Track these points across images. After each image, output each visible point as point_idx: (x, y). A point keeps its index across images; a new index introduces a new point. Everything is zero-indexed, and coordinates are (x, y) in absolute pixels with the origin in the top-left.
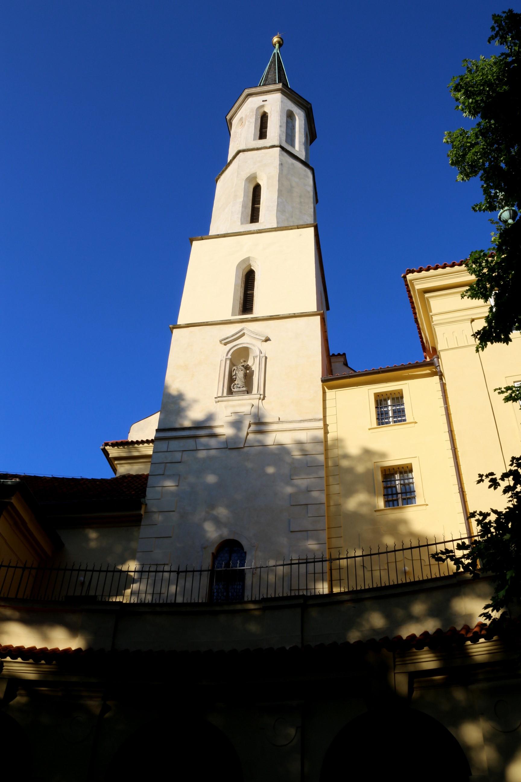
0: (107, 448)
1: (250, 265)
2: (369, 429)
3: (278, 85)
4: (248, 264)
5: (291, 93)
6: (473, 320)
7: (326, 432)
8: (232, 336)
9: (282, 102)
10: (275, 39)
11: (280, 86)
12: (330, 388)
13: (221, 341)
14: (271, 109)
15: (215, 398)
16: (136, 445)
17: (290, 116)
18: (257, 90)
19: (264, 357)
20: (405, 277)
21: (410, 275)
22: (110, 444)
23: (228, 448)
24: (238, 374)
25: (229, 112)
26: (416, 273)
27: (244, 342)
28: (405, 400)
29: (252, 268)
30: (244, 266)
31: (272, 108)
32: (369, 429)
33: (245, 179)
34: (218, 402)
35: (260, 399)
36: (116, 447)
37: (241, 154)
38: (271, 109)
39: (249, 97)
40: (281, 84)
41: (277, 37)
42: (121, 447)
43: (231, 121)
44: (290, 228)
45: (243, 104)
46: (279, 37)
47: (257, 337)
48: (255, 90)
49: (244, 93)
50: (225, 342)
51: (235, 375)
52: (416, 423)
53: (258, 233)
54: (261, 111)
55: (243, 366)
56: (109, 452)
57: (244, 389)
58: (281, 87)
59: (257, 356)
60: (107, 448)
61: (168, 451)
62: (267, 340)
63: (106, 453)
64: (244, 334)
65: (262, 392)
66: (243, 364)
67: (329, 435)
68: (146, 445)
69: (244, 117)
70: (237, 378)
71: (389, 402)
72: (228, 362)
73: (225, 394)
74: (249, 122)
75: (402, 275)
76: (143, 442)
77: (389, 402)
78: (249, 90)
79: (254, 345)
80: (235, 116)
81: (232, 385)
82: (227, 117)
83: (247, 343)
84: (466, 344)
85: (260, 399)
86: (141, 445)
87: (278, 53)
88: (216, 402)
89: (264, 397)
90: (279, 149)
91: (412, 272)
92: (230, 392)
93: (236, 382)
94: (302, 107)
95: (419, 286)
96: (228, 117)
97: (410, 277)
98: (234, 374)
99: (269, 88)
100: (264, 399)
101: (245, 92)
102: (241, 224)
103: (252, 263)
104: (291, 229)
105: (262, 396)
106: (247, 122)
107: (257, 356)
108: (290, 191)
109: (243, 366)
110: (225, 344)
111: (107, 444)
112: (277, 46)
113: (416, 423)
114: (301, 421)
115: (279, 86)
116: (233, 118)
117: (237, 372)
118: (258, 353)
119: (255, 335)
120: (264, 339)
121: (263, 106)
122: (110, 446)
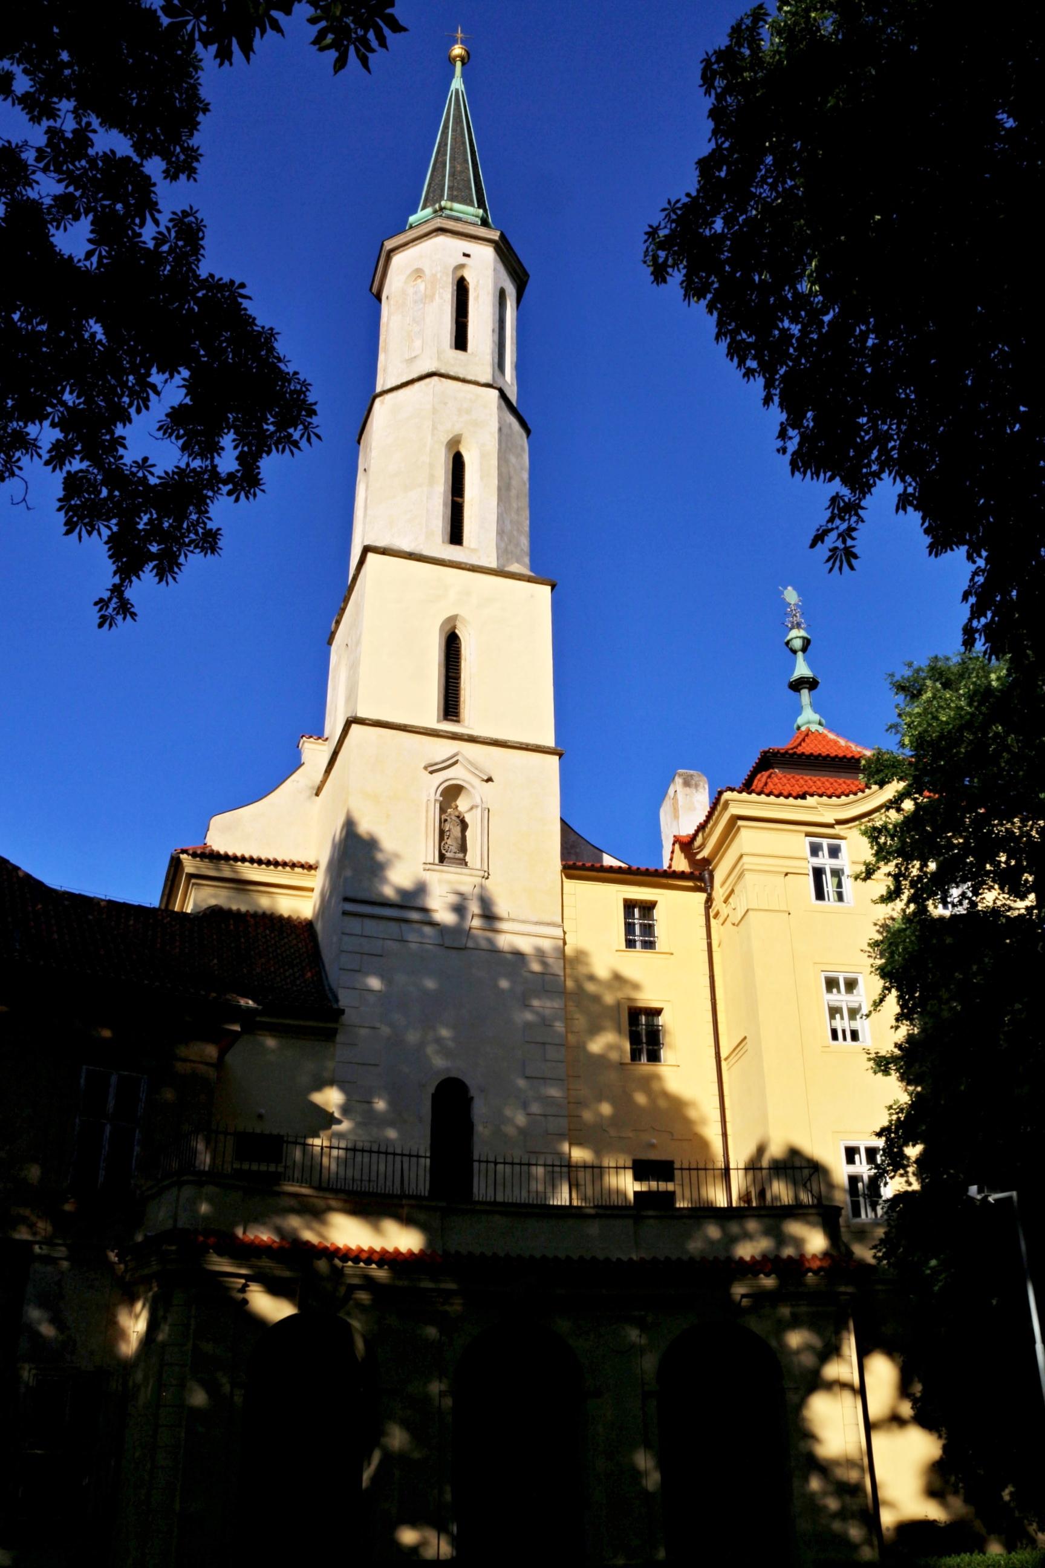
0: (183, 856)
1: (455, 627)
2: (617, 951)
3: (493, 233)
4: (452, 625)
5: (508, 250)
6: (786, 874)
7: (565, 943)
8: (443, 762)
9: (495, 270)
10: (457, 50)
11: (496, 235)
12: (569, 877)
13: (426, 768)
14: (478, 282)
15: (424, 863)
16: (232, 862)
17: (502, 295)
18: (458, 227)
19: (487, 810)
20: (720, 793)
21: (729, 793)
22: (191, 852)
23: (446, 945)
24: (453, 830)
25: (392, 237)
26: (735, 793)
27: (457, 775)
28: (657, 913)
29: (457, 631)
30: (448, 628)
31: (481, 282)
32: (617, 951)
33: (445, 443)
34: (428, 870)
35: (483, 877)
36: (198, 859)
37: (436, 378)
38: (478, 282)
39: (439, 232)
40: (498, 233)
41: (462, 48)
42: (207, 860)
43: (392, 254)
44: (518, 577)
45: (425, 238)
46: (465, 50)
47: (477, 772)
48: (454, 226)
49: (433, 223)
50: (433, 769)
51: (449, 831)
52: (672, 954)
53: (469, 570)
54: (459, 274)
55: (458, 817)
56: (185, 864)
57: (461, 855)
58: (497, 238)
59: (477, 806)
60: (183, 856)
61: (364, 934)
62: (489, 780)
63: (176, 864)
64: (456, 762)
65: (486, 869)
66: (457, 814)
67: (566, 947)
68: (247, 864)
69: (427, 272)
70: (451, 836)
71: (636, 911)
72: (438, 805)
73: (437, 861)
74: (441, 298)
75: (719, 790)
76: (243, 859)
77: (636, 911)
78: (444, 221)
79: (473, 787)
80: (401, 249)
81: (442, 844)
82: (386, 243)
83: (464, 780)
84: (778, 909)
85: (483, 877)
86: (239, 863)
87: (462, 91)
88: (424, 870)
89: (489, 874)
90: (496, 393)
91: (732, 790)
92: (442, 858)
93: (449, 842)
94: (515, 277)
95: (734, 810)
96: (389, 244)
97: (727, 795)
98: (447, 829)
99: (477, 231)
100: (487, 878)
101: (435, 221)
102: (443, 542)
103: (459, 625)
104: (519, 580)
105: (486, 874)
106: (437, 296)
107: (477, 806)
108: (508, 487)
109: (458, 817)
110: (431, 772)
111: (184, 851)
112: (459, 64)
113: (672, 954)
114: (537, 923)
115: (494, 235)
116: (397, 251)
117: (452, 827)
118: (478, 801)
119: (474, 767)
120: (486, 778)
121: (462, 266)
122: (188, 854)
